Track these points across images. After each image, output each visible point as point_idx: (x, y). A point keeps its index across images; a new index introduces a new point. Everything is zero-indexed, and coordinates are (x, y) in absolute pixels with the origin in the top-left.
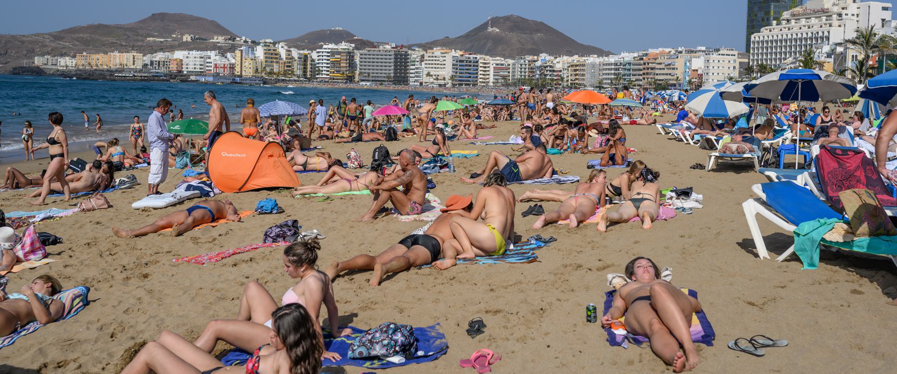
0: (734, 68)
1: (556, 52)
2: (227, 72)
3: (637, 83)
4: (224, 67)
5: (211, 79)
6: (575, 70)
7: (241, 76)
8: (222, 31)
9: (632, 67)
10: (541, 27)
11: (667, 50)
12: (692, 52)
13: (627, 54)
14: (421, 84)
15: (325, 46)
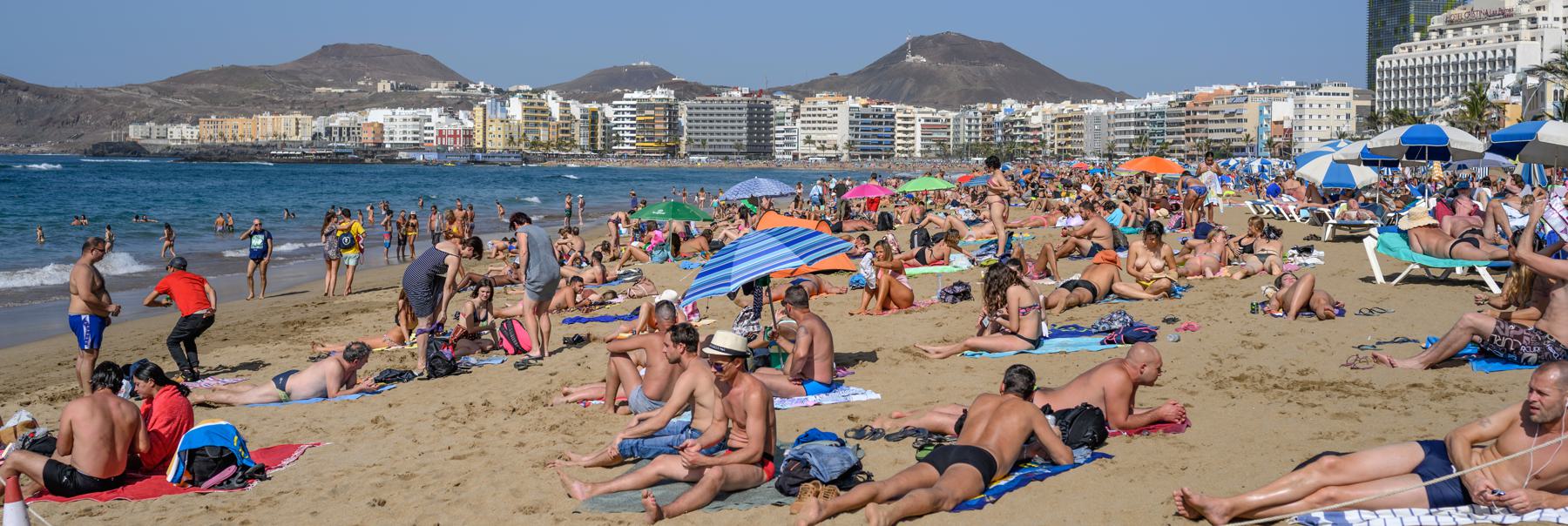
0: (1348, 116)
1: (1030, 95)
2: (460, 143)
3: (1176, 146)
4: (455, 136)
5: (433, 156)
6: (1066, 127)
7: (483, 150)
8: (444, 73)
9: (1166, 119)
10: (999, 52)
11: (1228, 88)
12: (1272, 90)
13: (1157, 97)
14: (795, 157)
15: (626, 96)
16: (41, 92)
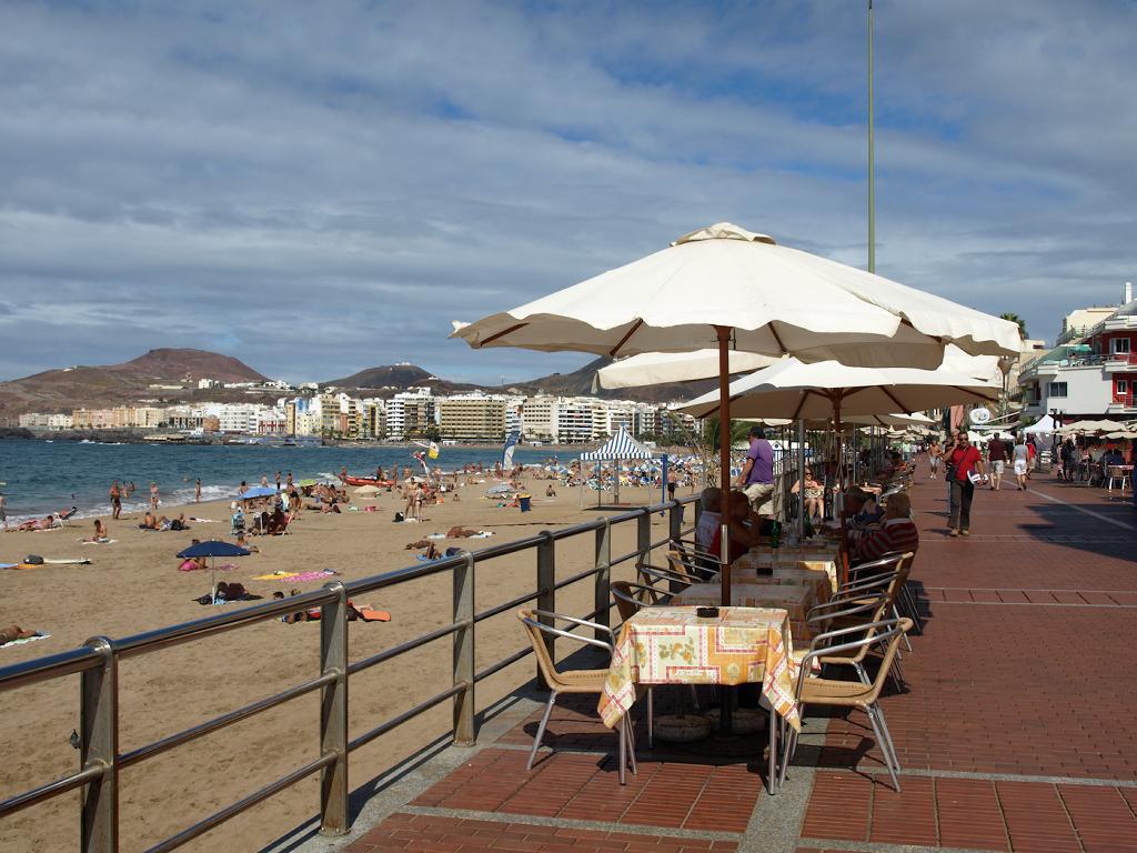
7: (293, 436)
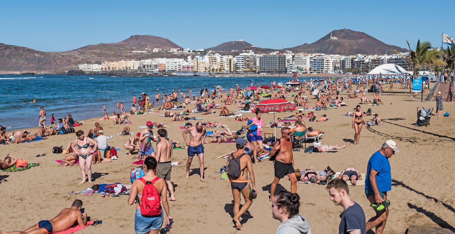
4: (188, 68)
16: (42, 53)
